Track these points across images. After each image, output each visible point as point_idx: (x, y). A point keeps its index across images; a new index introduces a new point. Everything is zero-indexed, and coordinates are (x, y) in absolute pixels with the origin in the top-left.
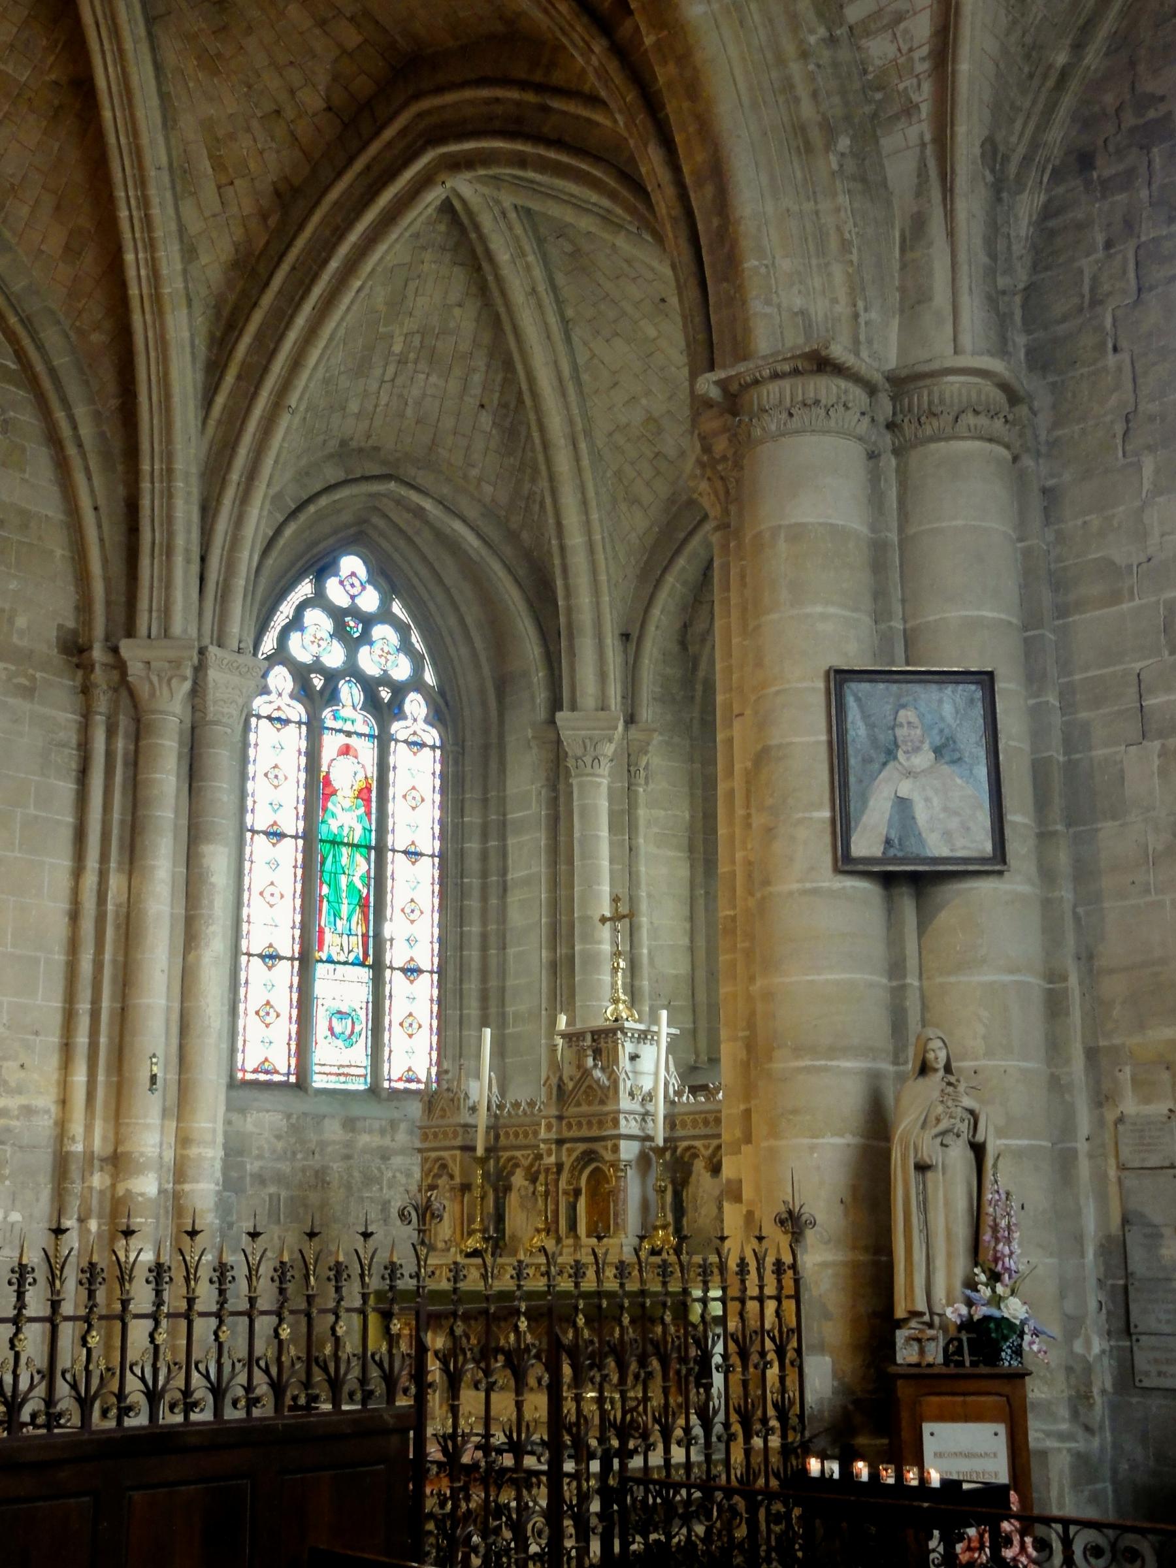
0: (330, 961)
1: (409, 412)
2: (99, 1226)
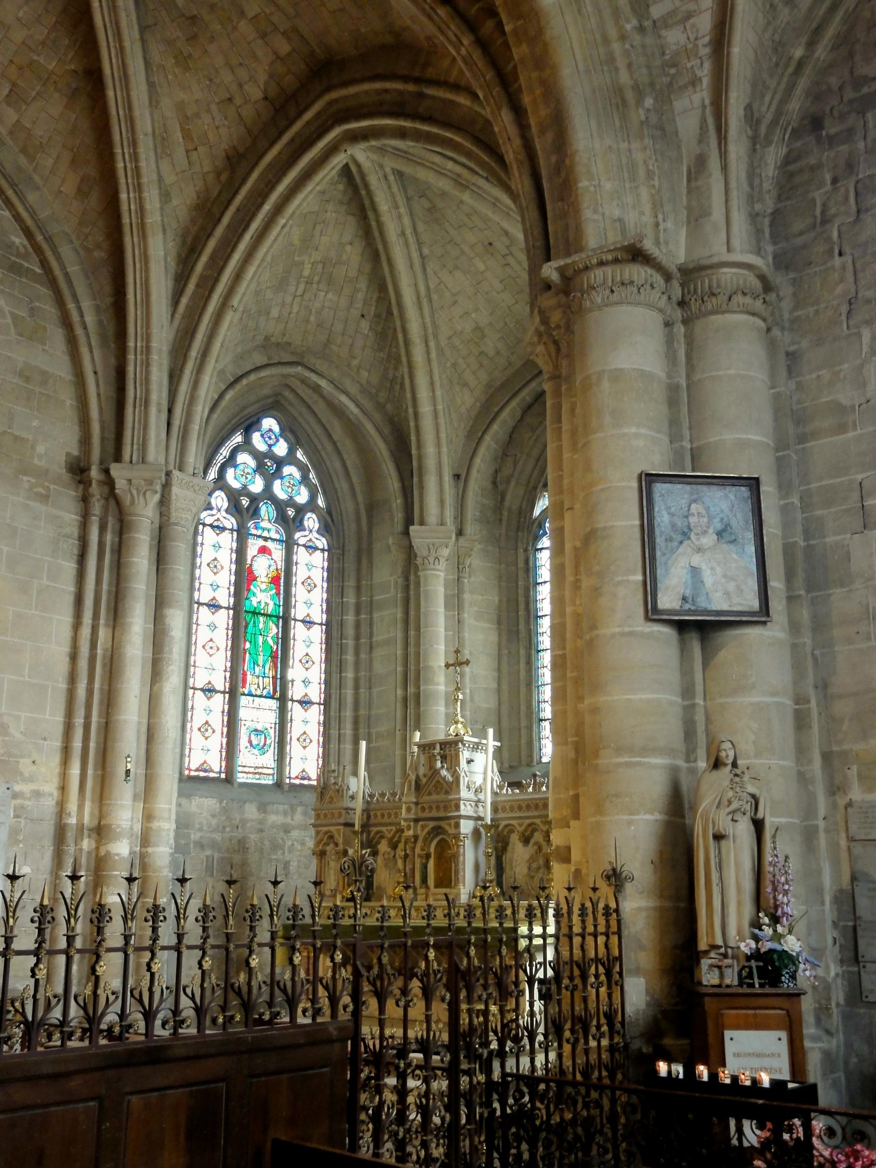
0: (250, 694)
1: (312, 318)
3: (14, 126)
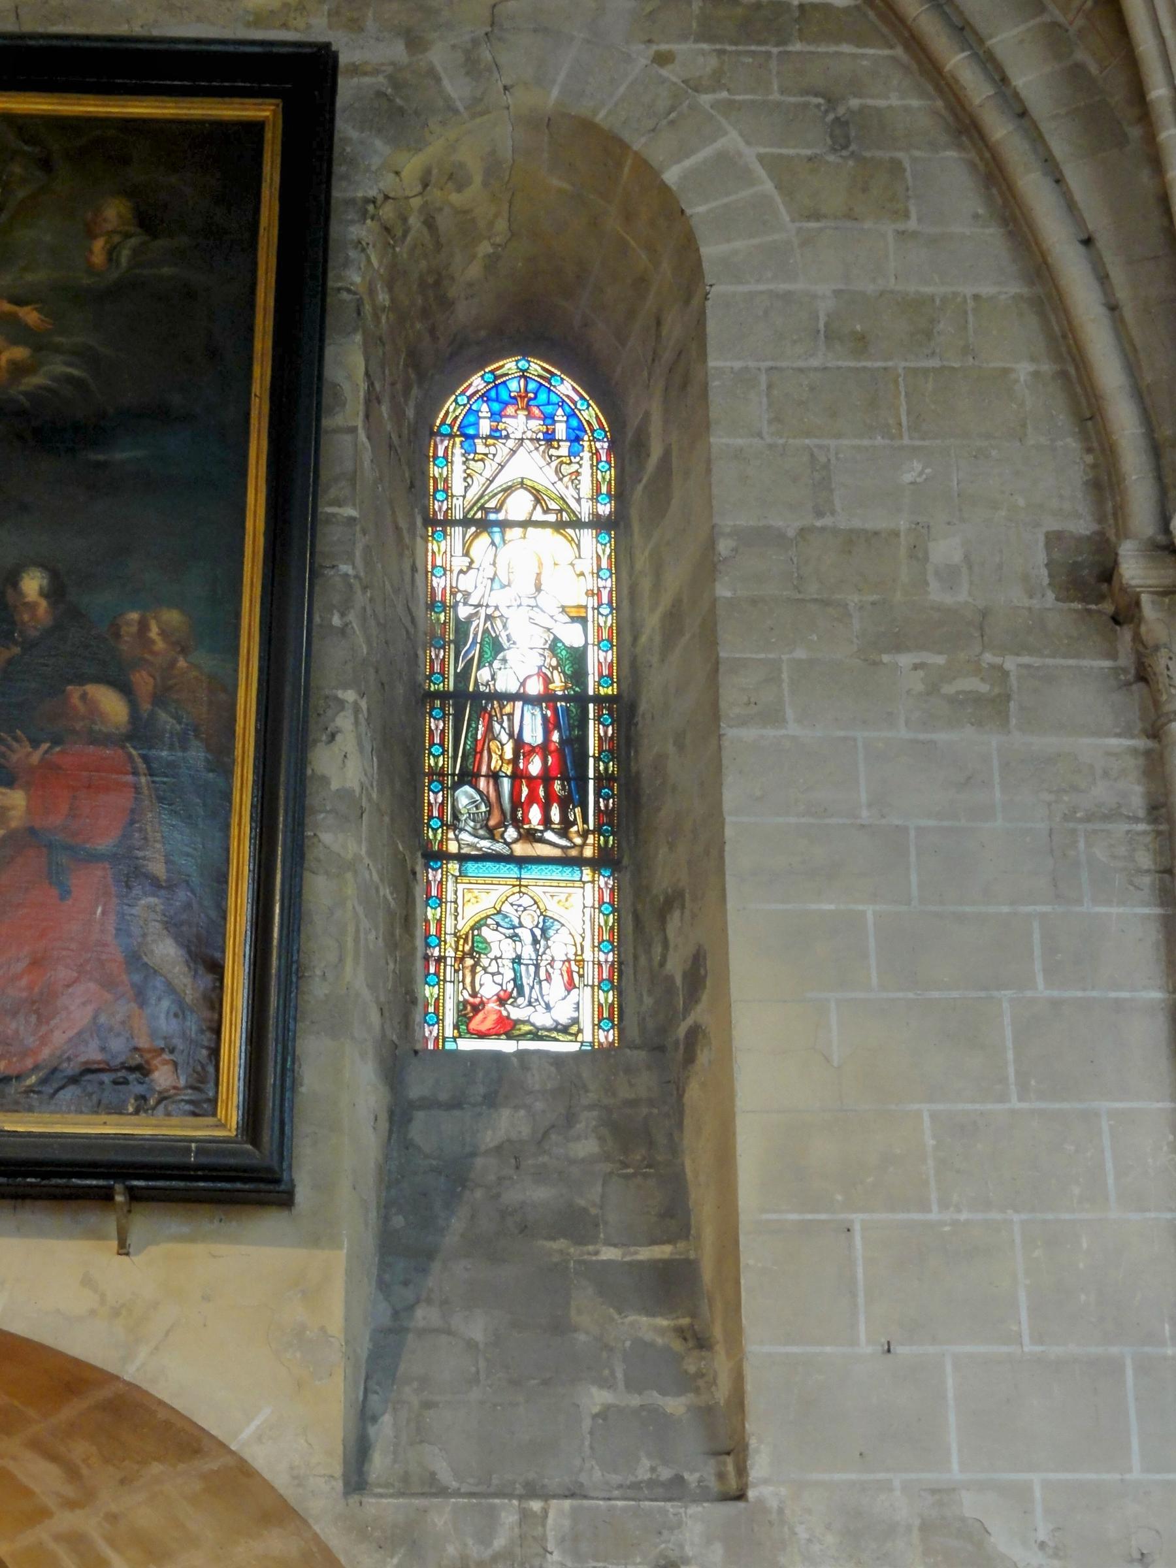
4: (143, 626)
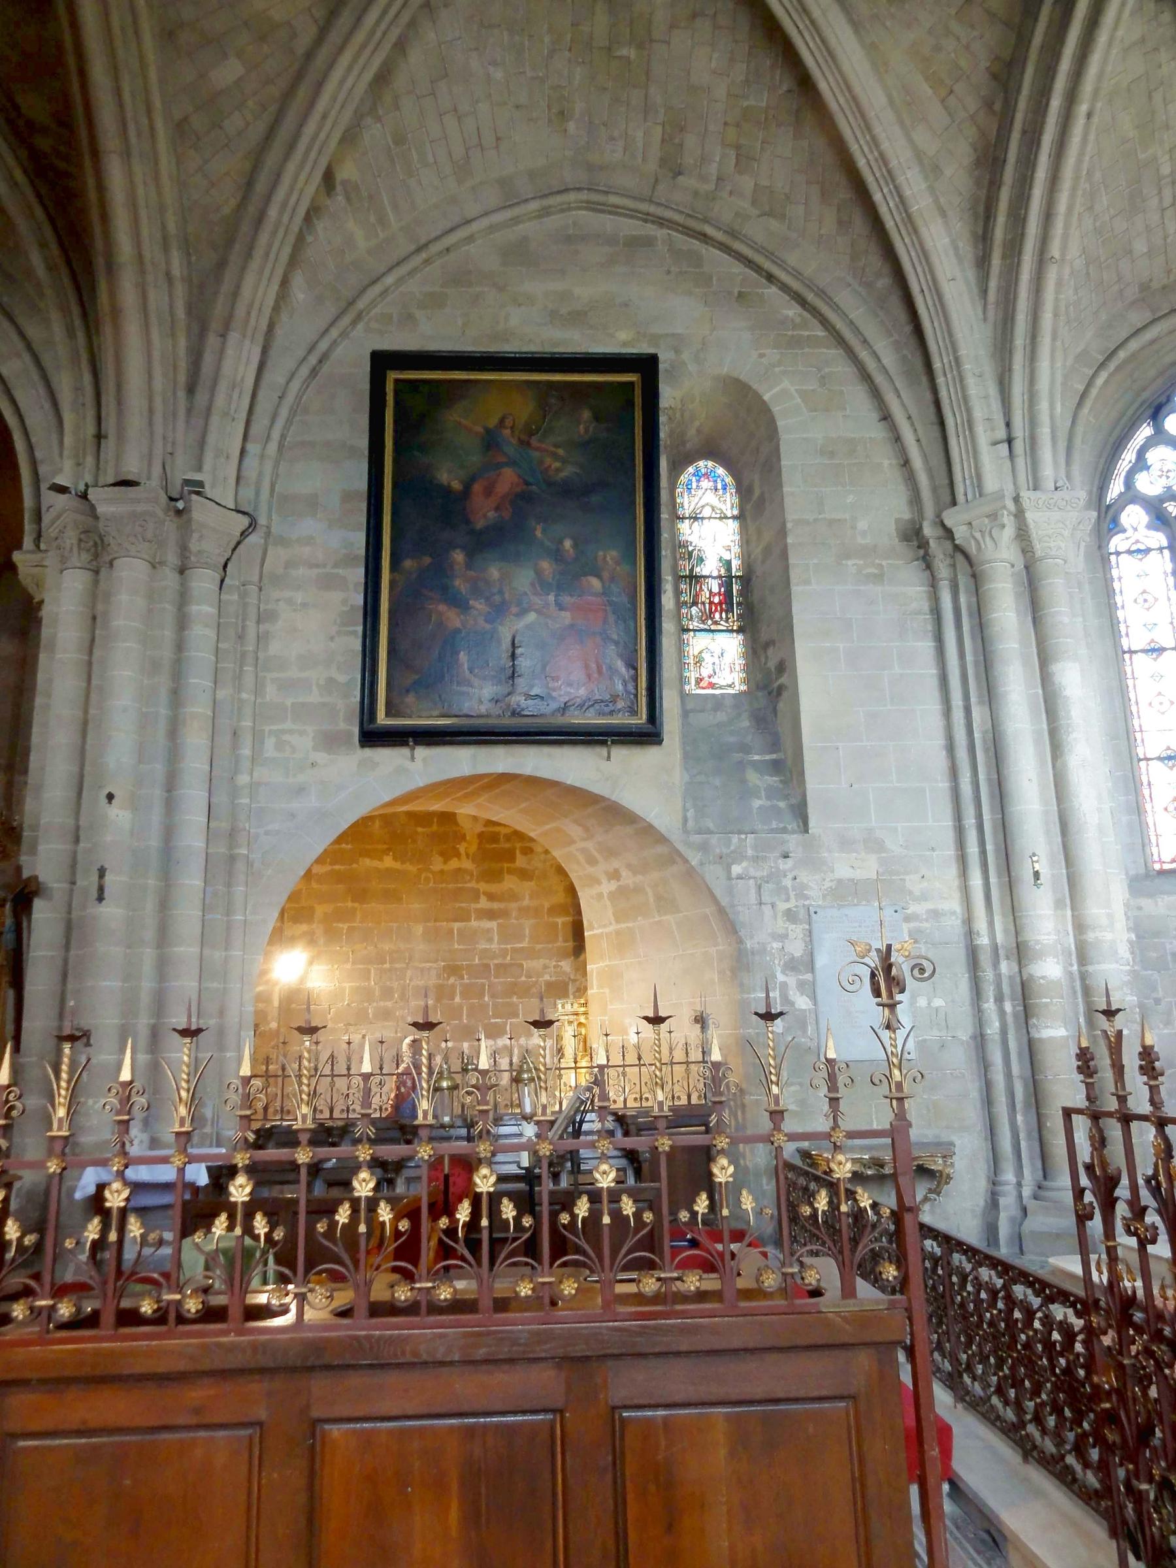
2: (1014, 1007)
3: (755, 191)
4: (605, 557)
